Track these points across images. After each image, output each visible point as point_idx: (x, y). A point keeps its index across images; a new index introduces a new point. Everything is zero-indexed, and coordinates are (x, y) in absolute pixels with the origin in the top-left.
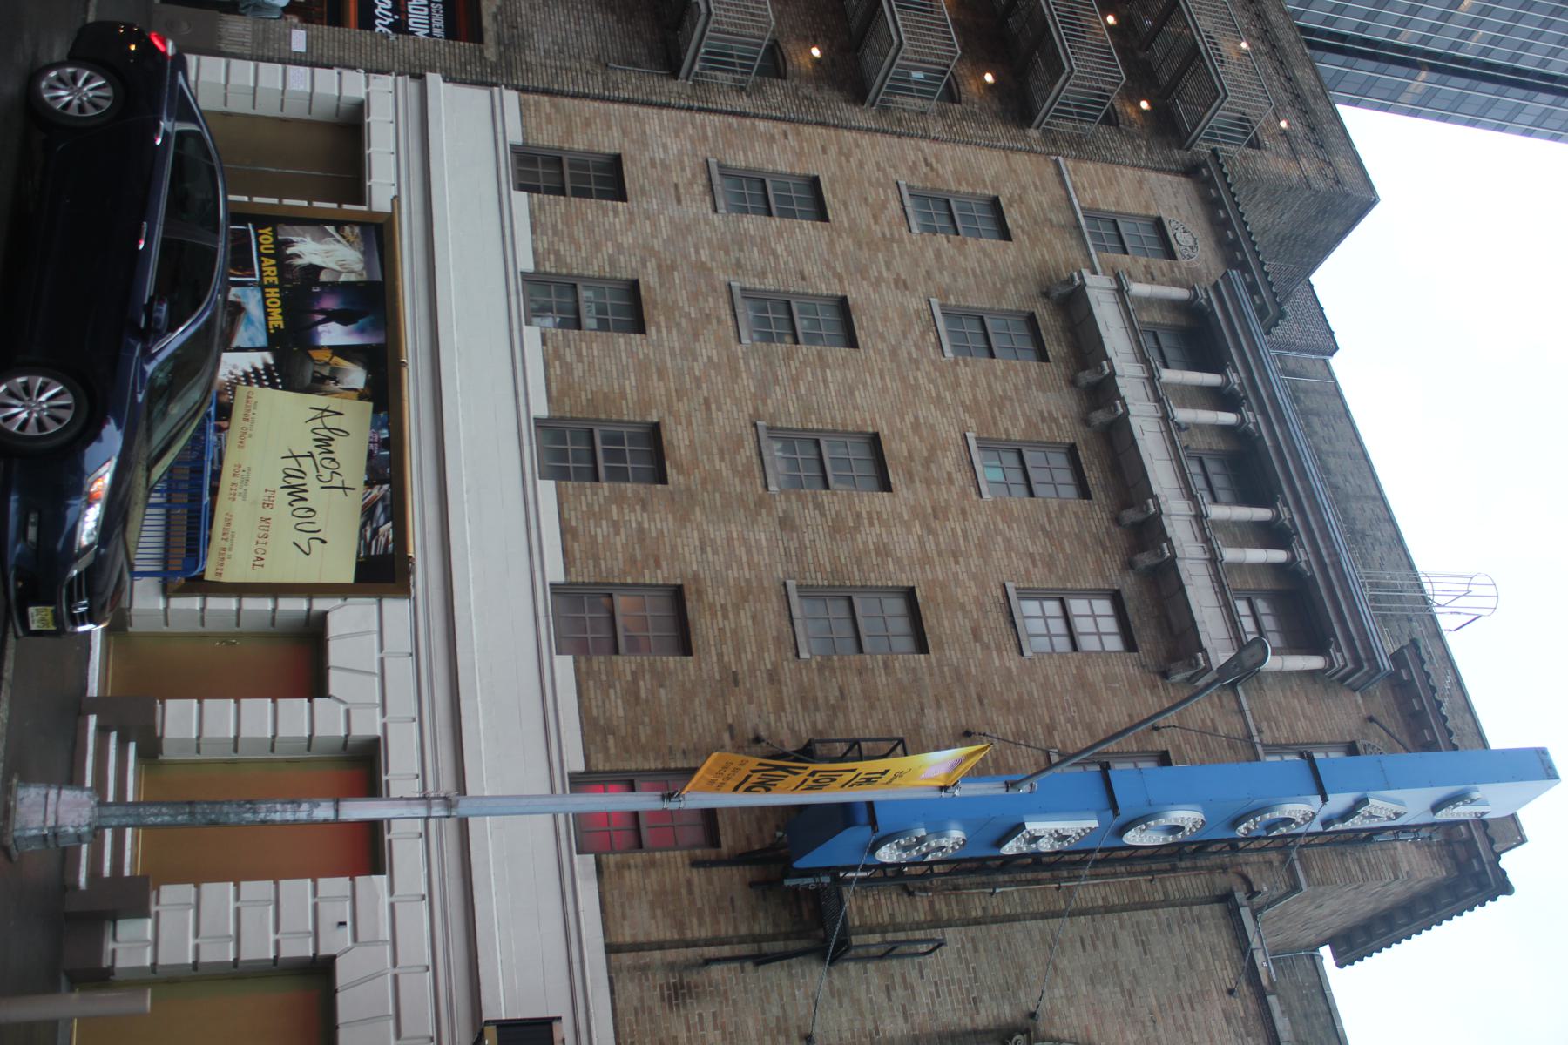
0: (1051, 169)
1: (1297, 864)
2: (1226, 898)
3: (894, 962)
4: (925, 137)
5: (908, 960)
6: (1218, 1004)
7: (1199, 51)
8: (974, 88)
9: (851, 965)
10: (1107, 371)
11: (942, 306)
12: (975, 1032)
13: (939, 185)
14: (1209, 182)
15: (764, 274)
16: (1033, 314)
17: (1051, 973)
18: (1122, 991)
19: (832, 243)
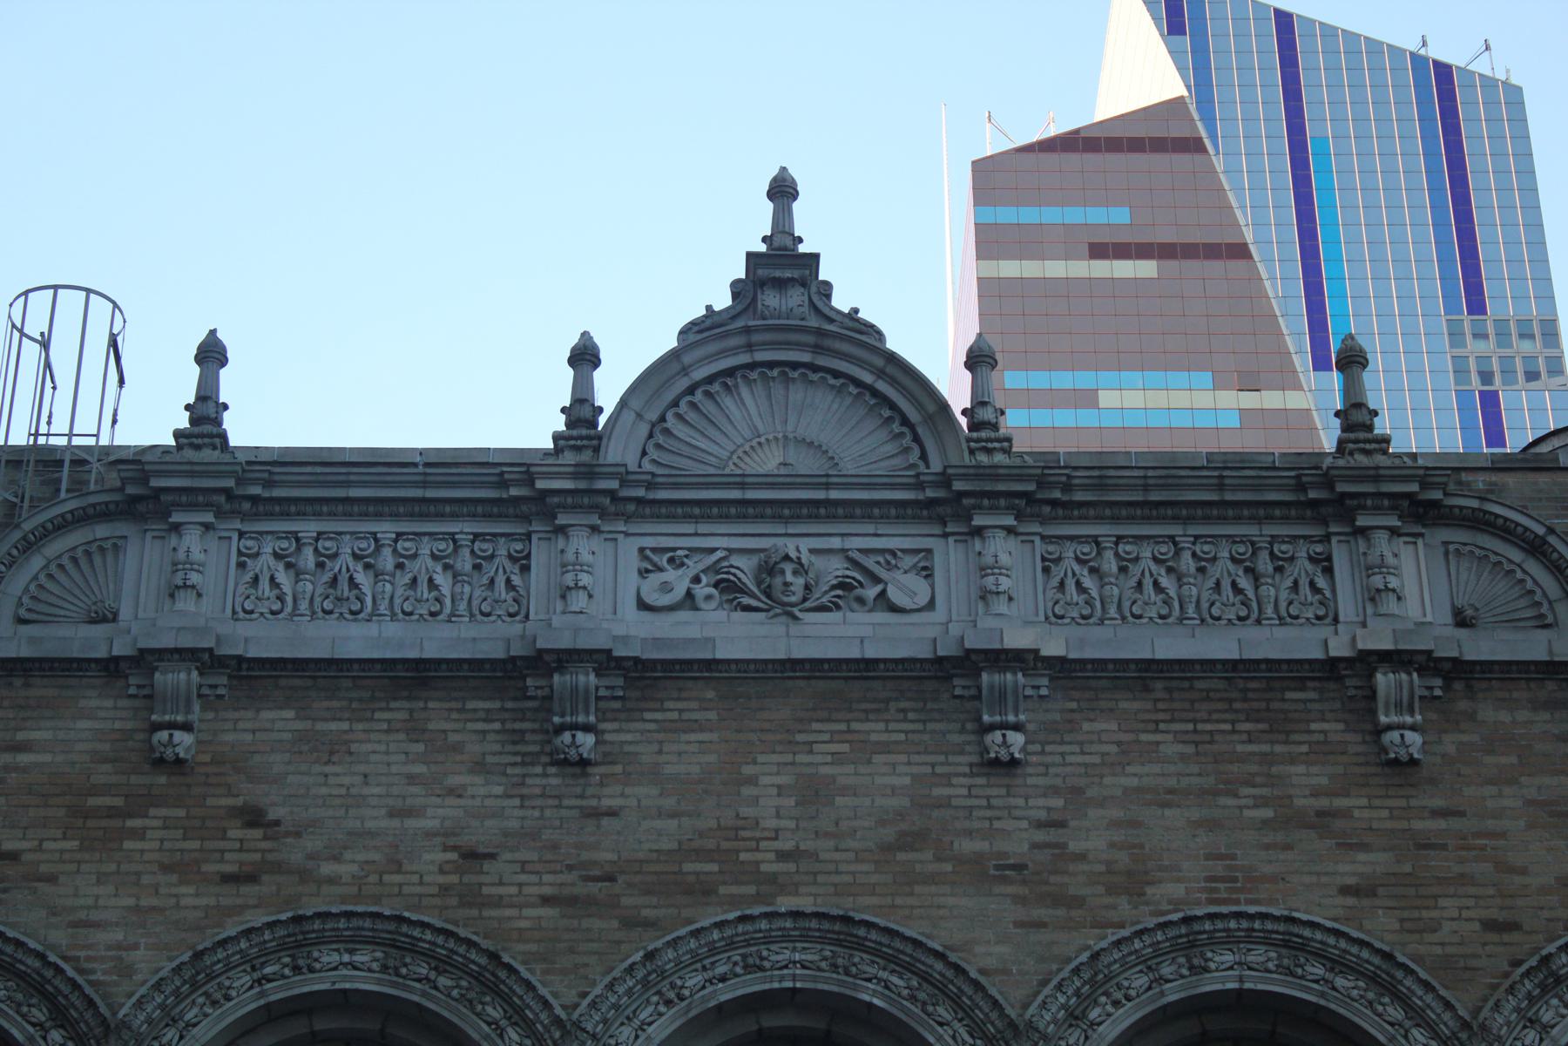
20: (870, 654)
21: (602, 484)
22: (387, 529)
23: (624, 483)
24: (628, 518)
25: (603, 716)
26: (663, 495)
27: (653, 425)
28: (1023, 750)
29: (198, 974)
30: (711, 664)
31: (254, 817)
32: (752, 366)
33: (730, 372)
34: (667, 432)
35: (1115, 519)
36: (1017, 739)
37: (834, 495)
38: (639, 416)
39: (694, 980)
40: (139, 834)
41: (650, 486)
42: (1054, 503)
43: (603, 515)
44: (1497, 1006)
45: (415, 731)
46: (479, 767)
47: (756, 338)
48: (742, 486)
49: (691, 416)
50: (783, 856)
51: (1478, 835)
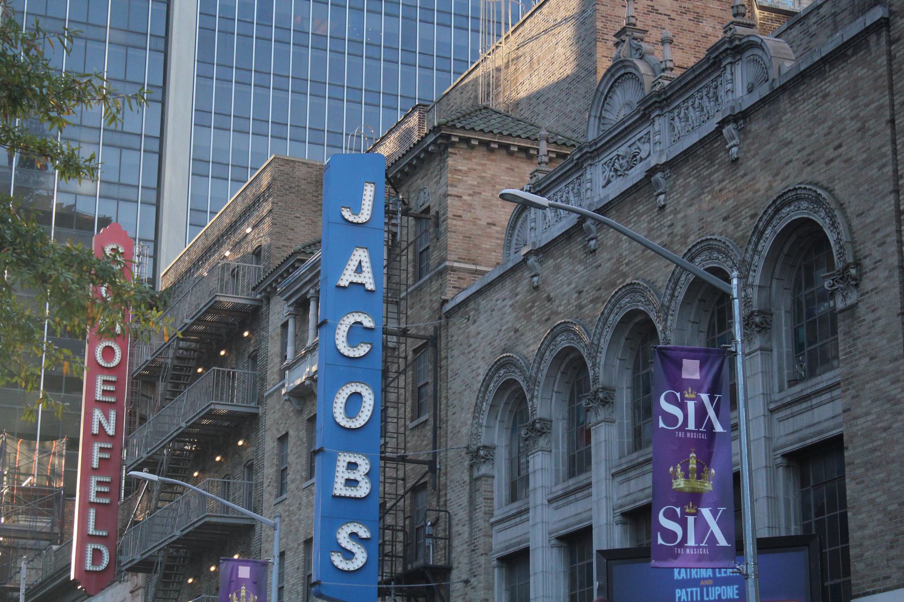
0: (269, 401)
1: (440, 267)
2: (449, 315)
3: (454, 530)
4: (262, 483)
5: (454, 522)
6: (473, 329)
7: (210, 308)
8: (249, 450)
9: (453, 555)
10: (307, 382)
11: (307, 480)
12: (470, 483)
13: (274, 478)
14: (265, 290)
15: (297, 592)
16: (308, 420)
17: (459, 435)
18: (465, 390)
19: (290, 549)
20: (635, 182)
21: (584, 151)
22: (562, 186)
23: (590, 146)
24: (598, 155)
25: (598, 231)
26: (599, 145)
27: (600, 118)
28: (665, 200)
29: (541, 354)
30: (610, 203)
31: (549, 299)
32: (615, 81)
33: (612, 87)
34: (604, 118)
35: (681, 95)
36: (662, 197)
37: (627, 124)
38: (595, 117)
39: (612, 317)
40: (533, 314)
41: (596, 144)
42: (665, 99)
43: (593, 158)
44: (747, 249)
45: (570, 254)
46: (580, 262)
47: (613, 71)
48: (611, 133)
49: (608, 108)
50: (627, 264)
51: (750, 181)
